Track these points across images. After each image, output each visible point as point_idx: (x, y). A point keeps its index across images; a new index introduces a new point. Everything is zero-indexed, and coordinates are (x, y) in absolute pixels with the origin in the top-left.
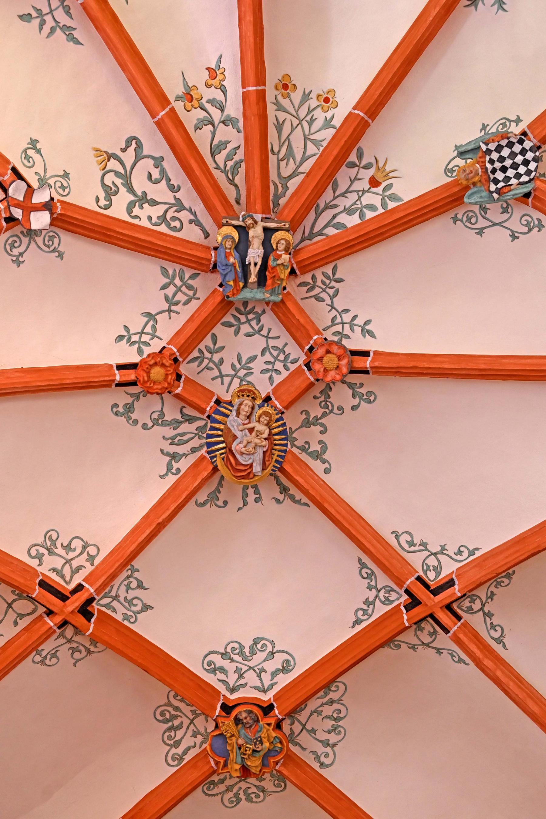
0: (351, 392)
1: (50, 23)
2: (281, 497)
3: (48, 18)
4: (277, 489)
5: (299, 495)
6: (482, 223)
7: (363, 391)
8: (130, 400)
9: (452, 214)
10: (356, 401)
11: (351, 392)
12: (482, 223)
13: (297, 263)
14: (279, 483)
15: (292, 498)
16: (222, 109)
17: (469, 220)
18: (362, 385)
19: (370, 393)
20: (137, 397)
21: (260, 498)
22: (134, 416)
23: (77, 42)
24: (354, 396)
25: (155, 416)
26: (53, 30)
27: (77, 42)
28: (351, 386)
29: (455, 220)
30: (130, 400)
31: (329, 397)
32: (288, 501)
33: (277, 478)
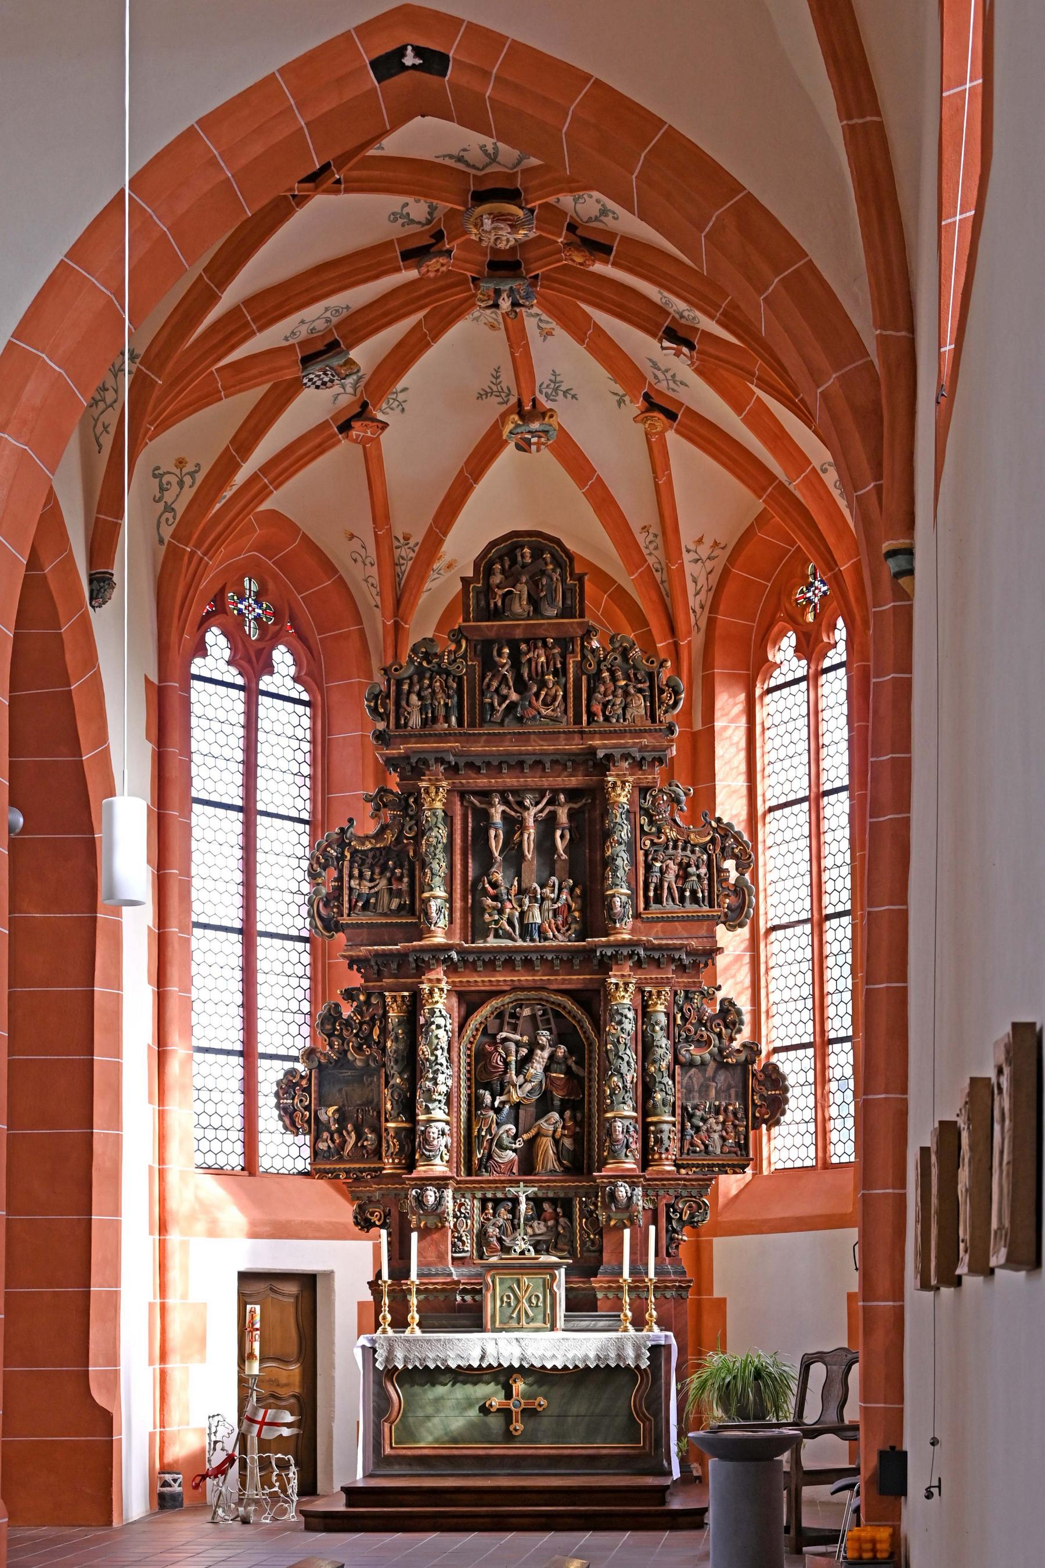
0: (411, 217)
1: (669, 375)
2: (462, 153)
3: (669, 377)
4: (466, 158)
5: (448, 162)
6: (328, 314)
7: (400, 221)
8: (602, 218)
9: (351, 311)
10: (405, 211)
11: (411, 217)
12: (328, 314)
13: (469, 289)
14: (468, 164)
15: (451, 157)
16: (540, 320)
17: (337, 311)
18: (403, 225)
19: (395, 220)
20: (597, 219)
21: (481, 148)
22: (599, 206)
23: (650, 360)
24: (408, 214)
25: (581, 201)
26: (667, 371)
27: (650, 360)
28: (412, 221)
29: (348, 307)
30: (602, 218)
31: (429, 207)
32: (455, 152)
33: (468, 164)
